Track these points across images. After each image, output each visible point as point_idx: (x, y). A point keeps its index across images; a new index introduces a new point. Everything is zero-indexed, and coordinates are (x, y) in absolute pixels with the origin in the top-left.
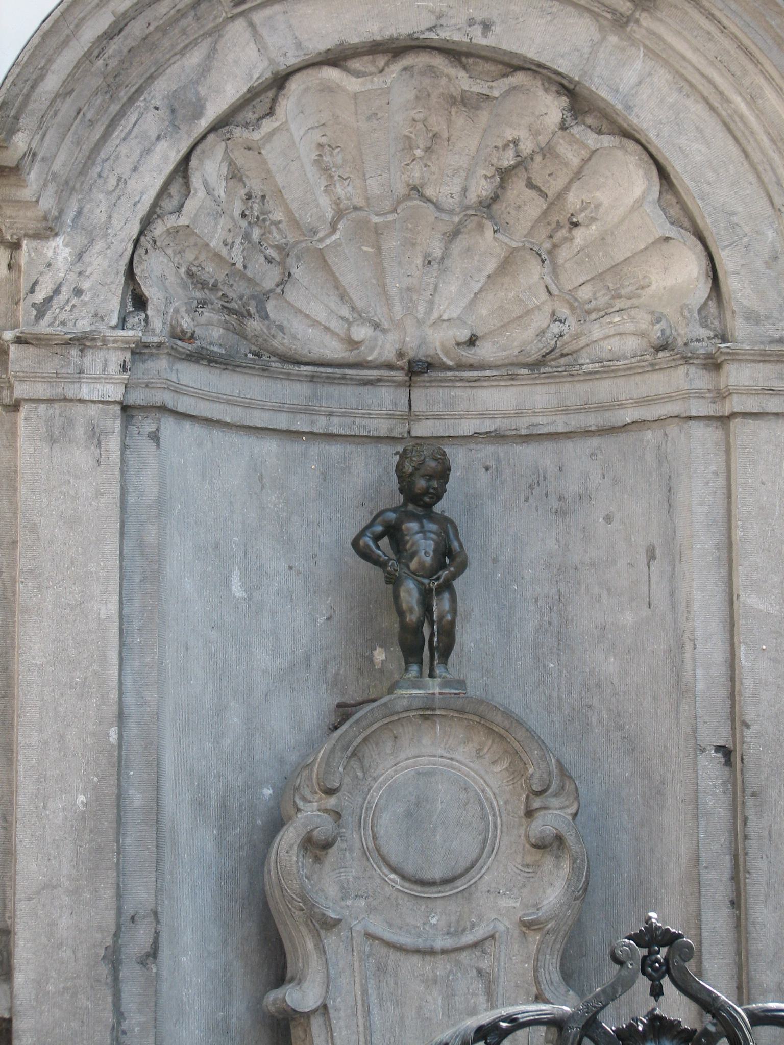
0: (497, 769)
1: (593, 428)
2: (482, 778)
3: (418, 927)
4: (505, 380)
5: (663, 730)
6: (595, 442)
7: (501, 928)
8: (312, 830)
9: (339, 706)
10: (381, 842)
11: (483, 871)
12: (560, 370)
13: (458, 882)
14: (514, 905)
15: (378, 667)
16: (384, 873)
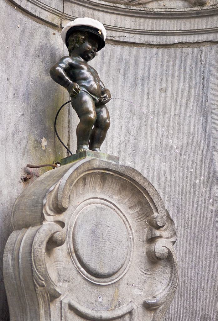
0: (131, 212)
1: (155, 43)
2: (124, 215)
3: (92, 303)
4: (111, 9)
5: (200, 203)
6: (154, 50)
7: (135, 307)
8: (54, 233)
9: (28, 166)
10: (79, 246)
11: (125, 271)
12: (141, 9)
13: (114, 277)
14: (140, 293)
15: (43, 149)
16: (78, 267)
